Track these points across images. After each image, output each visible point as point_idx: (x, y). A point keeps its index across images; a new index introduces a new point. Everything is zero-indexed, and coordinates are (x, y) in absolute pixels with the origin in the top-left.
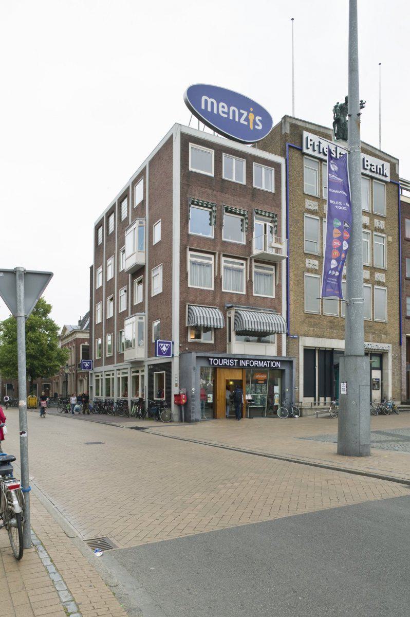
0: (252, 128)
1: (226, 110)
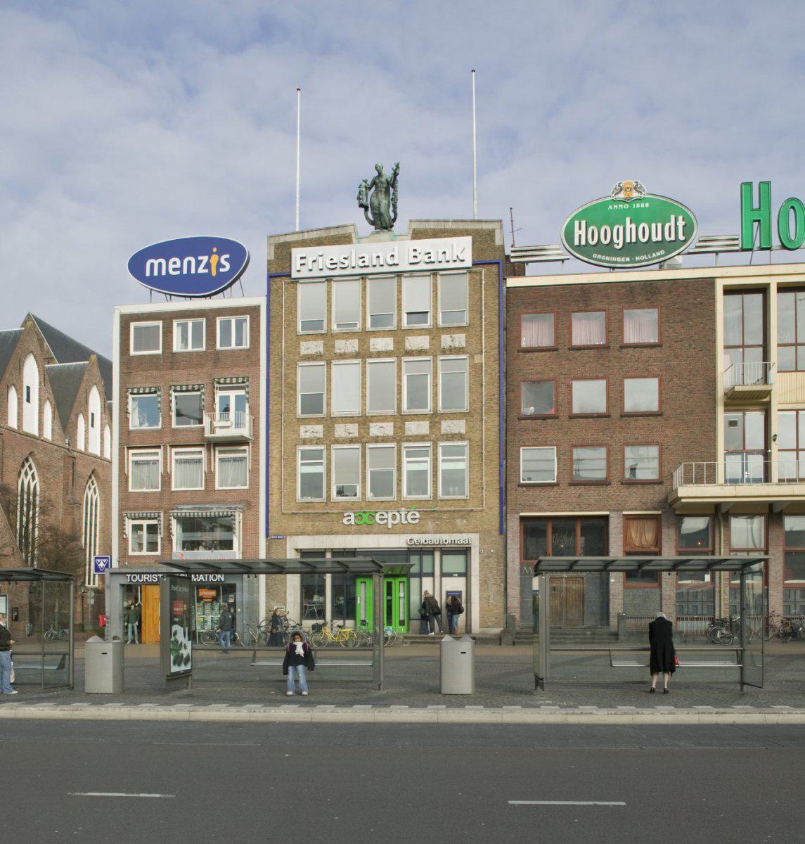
0: (214, 274)
1: (178, 265)
